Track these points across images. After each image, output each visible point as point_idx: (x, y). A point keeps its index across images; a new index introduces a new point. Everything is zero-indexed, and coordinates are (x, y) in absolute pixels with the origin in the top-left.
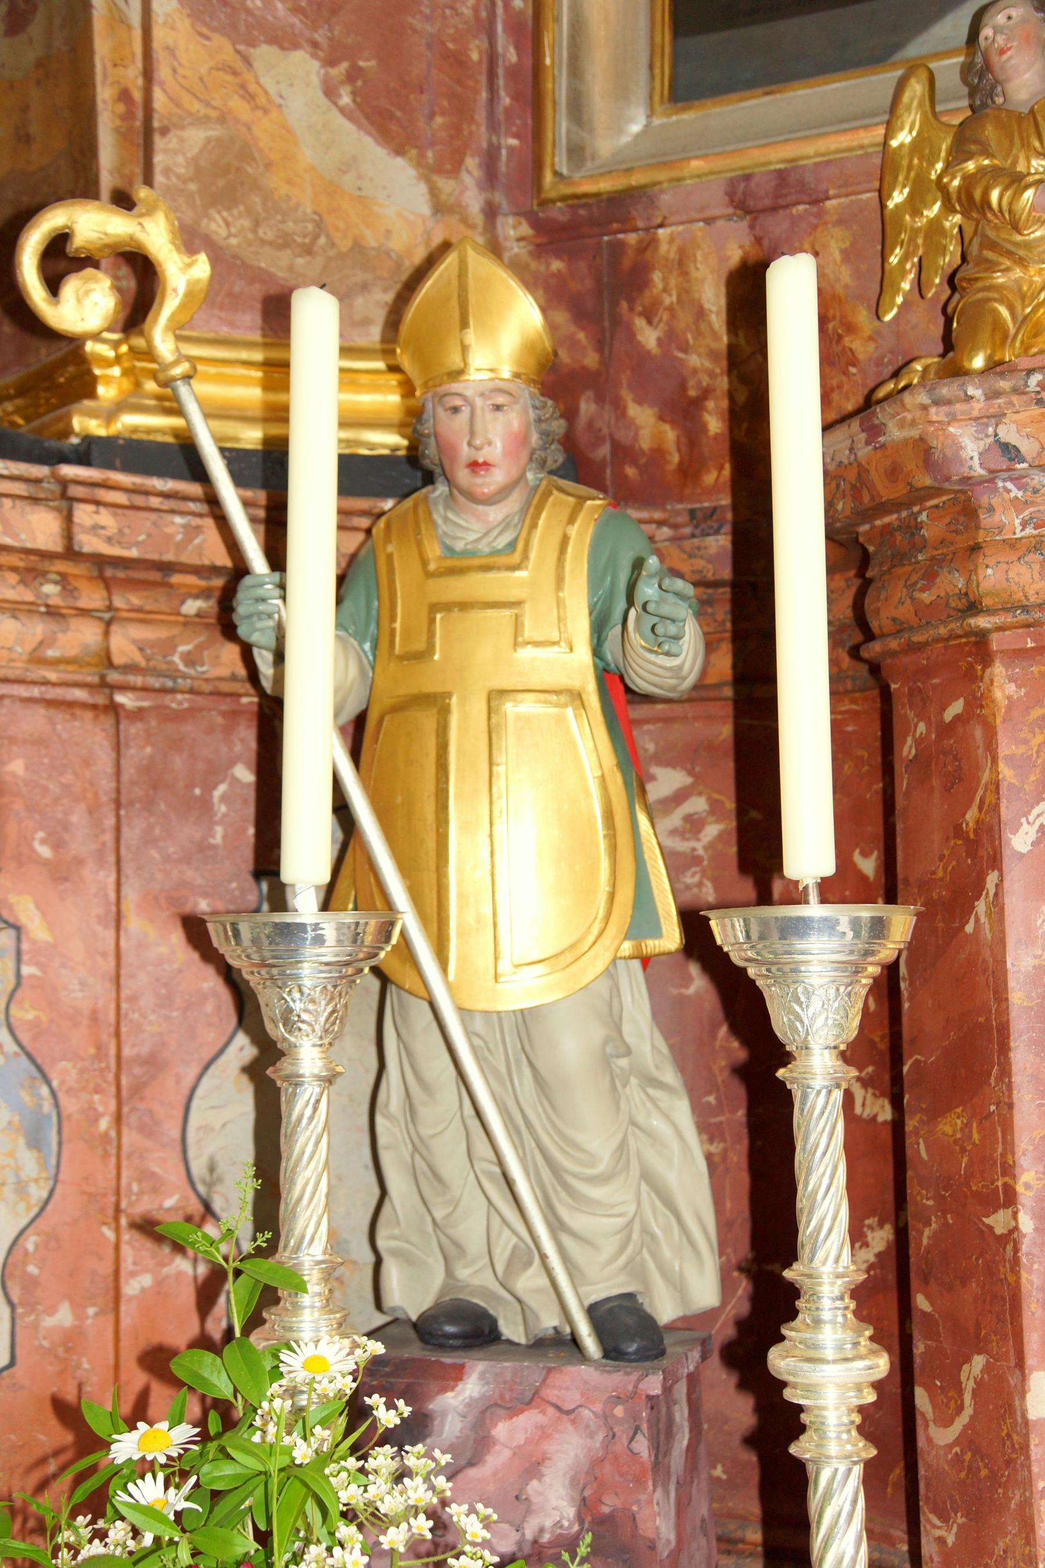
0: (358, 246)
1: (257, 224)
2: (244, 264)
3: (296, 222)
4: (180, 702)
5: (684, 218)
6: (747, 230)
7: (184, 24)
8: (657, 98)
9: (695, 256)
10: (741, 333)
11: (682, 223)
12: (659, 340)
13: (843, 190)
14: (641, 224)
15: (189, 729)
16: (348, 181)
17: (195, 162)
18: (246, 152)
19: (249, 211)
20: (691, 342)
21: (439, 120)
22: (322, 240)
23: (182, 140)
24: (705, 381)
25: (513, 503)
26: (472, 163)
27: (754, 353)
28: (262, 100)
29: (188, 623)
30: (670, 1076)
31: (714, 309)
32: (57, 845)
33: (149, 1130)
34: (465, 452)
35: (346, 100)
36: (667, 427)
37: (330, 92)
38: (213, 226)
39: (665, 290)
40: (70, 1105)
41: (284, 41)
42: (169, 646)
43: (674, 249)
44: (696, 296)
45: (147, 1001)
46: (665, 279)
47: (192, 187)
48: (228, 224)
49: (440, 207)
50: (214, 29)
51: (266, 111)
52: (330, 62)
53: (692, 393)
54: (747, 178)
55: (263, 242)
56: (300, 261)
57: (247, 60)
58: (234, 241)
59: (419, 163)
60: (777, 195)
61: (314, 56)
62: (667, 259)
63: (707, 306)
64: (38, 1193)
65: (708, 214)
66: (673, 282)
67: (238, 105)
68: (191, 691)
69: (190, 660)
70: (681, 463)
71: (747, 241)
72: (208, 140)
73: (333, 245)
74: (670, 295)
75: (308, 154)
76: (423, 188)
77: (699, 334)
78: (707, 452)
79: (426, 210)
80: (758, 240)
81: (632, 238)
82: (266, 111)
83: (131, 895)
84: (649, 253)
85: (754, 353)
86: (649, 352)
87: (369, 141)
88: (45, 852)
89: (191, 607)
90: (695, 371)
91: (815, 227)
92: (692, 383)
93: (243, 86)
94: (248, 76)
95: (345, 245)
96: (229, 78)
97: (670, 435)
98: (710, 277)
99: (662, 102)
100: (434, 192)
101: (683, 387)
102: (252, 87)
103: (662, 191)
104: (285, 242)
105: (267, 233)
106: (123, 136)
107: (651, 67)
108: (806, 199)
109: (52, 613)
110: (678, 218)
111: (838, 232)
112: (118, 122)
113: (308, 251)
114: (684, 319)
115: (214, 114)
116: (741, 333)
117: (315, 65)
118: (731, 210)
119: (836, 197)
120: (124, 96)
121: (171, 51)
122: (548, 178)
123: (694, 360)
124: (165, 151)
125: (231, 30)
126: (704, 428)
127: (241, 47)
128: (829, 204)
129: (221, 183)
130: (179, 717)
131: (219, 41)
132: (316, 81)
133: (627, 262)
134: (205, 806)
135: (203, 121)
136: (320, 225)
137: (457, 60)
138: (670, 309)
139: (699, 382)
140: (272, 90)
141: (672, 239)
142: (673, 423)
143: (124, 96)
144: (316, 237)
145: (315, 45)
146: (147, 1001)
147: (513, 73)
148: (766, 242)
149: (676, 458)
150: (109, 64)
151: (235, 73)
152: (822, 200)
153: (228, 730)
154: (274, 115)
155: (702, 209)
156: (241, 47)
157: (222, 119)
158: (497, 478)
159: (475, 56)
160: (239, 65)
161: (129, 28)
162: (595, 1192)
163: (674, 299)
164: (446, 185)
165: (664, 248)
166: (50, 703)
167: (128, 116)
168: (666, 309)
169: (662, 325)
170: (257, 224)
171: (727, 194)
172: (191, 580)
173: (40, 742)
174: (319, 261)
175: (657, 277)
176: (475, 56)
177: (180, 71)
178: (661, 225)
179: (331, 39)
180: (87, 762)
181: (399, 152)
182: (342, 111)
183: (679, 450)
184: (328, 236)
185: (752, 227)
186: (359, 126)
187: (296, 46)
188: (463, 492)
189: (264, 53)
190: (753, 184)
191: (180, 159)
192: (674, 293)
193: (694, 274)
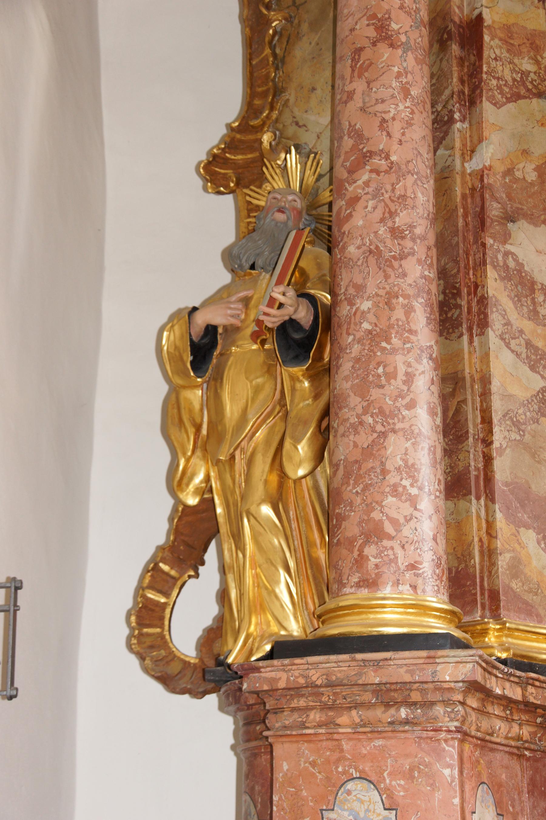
1: (523, 585)
2: (521, 598)
3: (533, 584)
4: (538, 755)
7: (504, 521)
17: (508, 564)
22: (540, 591)
23: (505, 557)
28: (522, 545)
35: (543, 546)
37: (539, 543)
38: (513, 585)
41: (527, 527)
47: (508, 572)
48: (516, 585)
50: (510, 523)
51: (524, 548)
52: (538, 534)
55: (525, 591)
56: (535, 597)
57: (518, 532)
58: (518, 590)
61: (534, 531)
67: (516, 545)
72: (511, 557)
75: (534, 563)
82: (524, 548)
89: (539, 720)
93: (518, 540)
94: (519, 537)
96: (514, 538)
102: (520, 541)
104: (530, 591)
105: (526, 588)
106: (482, 553)
113: (536, 594)
115: (511, 549)
117: (535, 534)
120: (481, 540)
121: (501, 529)
124: (501, 560)
127: (517, 528)
129: (514, 571)
131: (512, 526)
132: (535, 539)
135: (509, 551)
136: (538, 585)
140: (525, 542)
144: (538, 590)
145: (534, 528)
151: (516, 536)
154: (525, 549)
156: (517, 528)
157: (513, 551)
160: (516, 533)
161: (481, 519)
167: (482, 546)
170: (523, 585)
174: (539, 597)
177: (504, 535)
179: (538, 526)
182: (542, 549)
184: (542, 590)
187: (530, 529)
189: (522, 530)
191: (505, 563)
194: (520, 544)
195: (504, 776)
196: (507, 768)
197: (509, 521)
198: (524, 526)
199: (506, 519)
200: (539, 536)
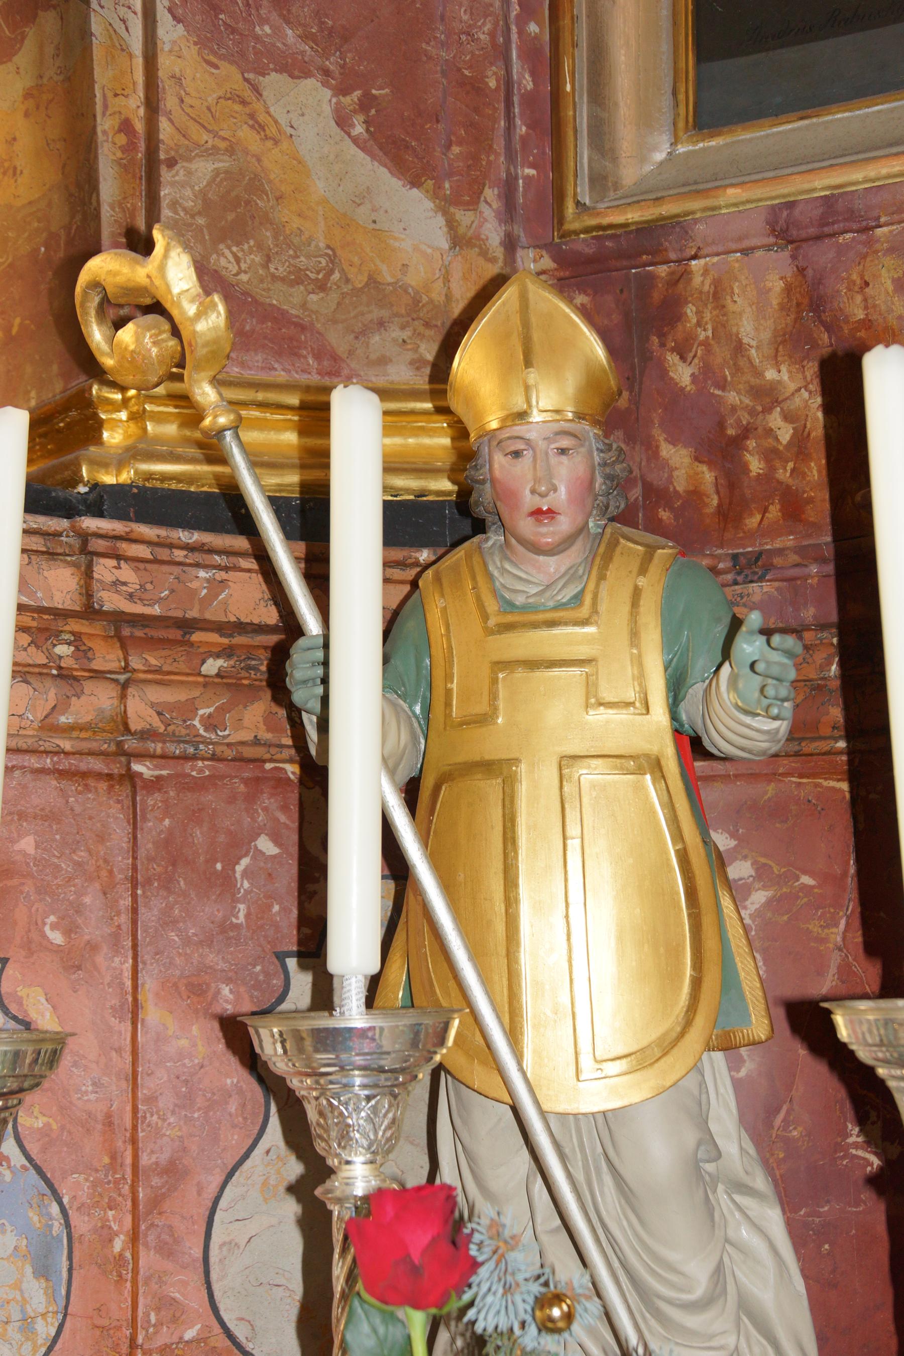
0: (373, 281)
1: (268, 259)
2: (256, 301)
3: (308, 257)
4: (200, 769)
5: (720, 249)
6: (790, 261)
7: (191, 52)
8: (681, 124)
9: (732, 289)
10: (784, 368)
11: (718, 254)
12: (693, 375)
13: (896, 217)
14: (673, 256)
15: (208, 798)
16: (363, 214)
17: (203, 194)
18: (256, 185)
19: (260, 246)
20: (729, 378)
21: (456, 150)
22: (336, 276)
23: (189, 173)
24: (745, 419)
25: (574, 555)
26: (490, 194)
27: (799, 390)
28: (272, 131)
29: (208, 683)
30: (761, 1182)
31: (754, 343)
32: (68, 932)
33: (167, 1250)
34: (529, 501)
35: (359, 129)
36: (704, 468)
37: (342, 121)
38: (223, 262)
39: (699, 324)
40: (82, 1224)
42: (190, 708)
43: (708, 282)
44: (734, 330)
45: (166, 1101)
46: (699, 313)
47: (201, 221)
48: (238, 260)
49: (458, 241)
50: (222, 57)
51: (276, 142)
52: (342, 90)
53: (731, 432)
54: (791, 205)
55: (274, 278)
56: (313, 297)
57: (257, 90)
58: (244, 277)
59: (435, 194)
60: (823, 221)
61: (325, 84)
62: (701, 292)
63: (745, 340)
64: (45, 1329)
65: (746, 244)
66: (707, 316)
67: (245, 134)
68: (214, 758)
69: (211, 724)
70: (720, 505)
71: (789, 272)
72: (217, 172)
73: (347, 281)
74: (705, 330)
75: (320, 186)
76: (440, 220)
77: (737, 369)
78: (748, 493)
79: (444, 244)
80: (801, 271)
81: (662, 270)
82: (276, 142)
83: (149, 983)
84: (681, 286)
85: (799, 390)
86: (682, 389)
87: (383, 173)
88: (56, 937)
89: (212, 666)
90: (734, 409)
91: (864, 257)
92: (731, 421)
93: (252, 116)
94: (257, 106)
95: (360, 280)
96: (237, 107)
97: (708, 476)
98: (748, 309)
99: (687, 129)
100: (451, 224)
101: (721, 425)
102: (262, 117)
103: (696, 221)
104: (297, 278)
105: (279, 268)
106: (126, 168)
107: (675, 93)
108: (855, 226)
109: (64, 676)
110: (714, 249)
111: (889, 261)
112: (119, 154)
113: (322, 287)
114: (721, 354)
115: (223, 145)
116: (784, 368)
117: (328, 93)
118: (772, 240)
119: (886, 224)
120: (126, 127)
121: (178, 79)
122: (570, 209)
123: (733, 397)
124: (173, 184)
125: (239, 58)
126: (746, 468)
127: (250, 76)
128: (879, 231)
129: (231, 216)
130: (199, 785)
131: (228, 69)
132: (327, 110)
133: (657, 296)
134: (227, 882)
135: (212, 152)
137: (475, 87)
138: (705, 343)
139: (739, 420)
140: (283, 121)
141: (706, 272)
142: (710, 464)
143: (126, 127)
144: (331, 272)
145: (327, 73)
146: (166, 1101)
147: (530, 100)
148: (810, 273)
149: (715, 502)
150: (110, 94)
151: (244, 103)
152: (873, 228)
153: (251, 799)
154: (285, 145)
155: (740, 239)
156: (250, 76)
157: (231, 151)
158: (564, 524)
159: (492, 84)
160: (248, 94)
161: (131, 56)
162: (692, 1321)
163: (710, 333)
164: (464, 217)
165: (697, 280)
166: (62, 774)
167: (130, 148)
168: (700, 344)
169: (696, 361)
170: (268, 259)
171: (767, 223)
172: (213, 637)
173: (50, 817)
174: (334, 296)
175: (690, 310)
176: (492, 84)
177: (187, 100)
178: (695, 257)
179: (343, 67)
180: (101, 838)
181: (415, 183)
182: (355, 141)
183: (718, 492)
184: (342, 271)
185: (794, 257)
186: (373, 157)
187: (307, 75)
188: (522, 541)
189: (274, 82)
190: (797, 212)
191: (188, 192)
192: (709, 327)
193: (731, 307)
194: (259, 127)
195: (27, 844)
196: (50, 817)
197: (215, 54)
198: (282, 68)
199: (202, 43)
200: (346, 100)
